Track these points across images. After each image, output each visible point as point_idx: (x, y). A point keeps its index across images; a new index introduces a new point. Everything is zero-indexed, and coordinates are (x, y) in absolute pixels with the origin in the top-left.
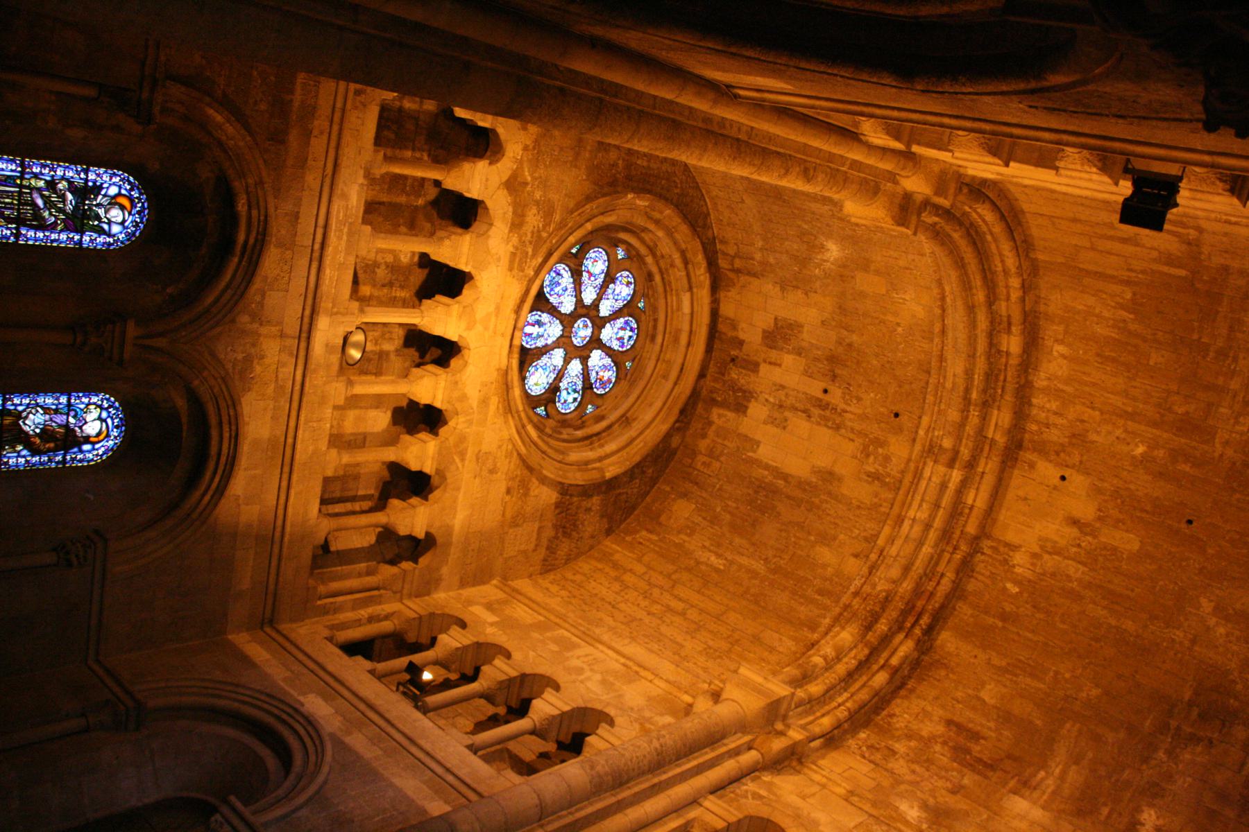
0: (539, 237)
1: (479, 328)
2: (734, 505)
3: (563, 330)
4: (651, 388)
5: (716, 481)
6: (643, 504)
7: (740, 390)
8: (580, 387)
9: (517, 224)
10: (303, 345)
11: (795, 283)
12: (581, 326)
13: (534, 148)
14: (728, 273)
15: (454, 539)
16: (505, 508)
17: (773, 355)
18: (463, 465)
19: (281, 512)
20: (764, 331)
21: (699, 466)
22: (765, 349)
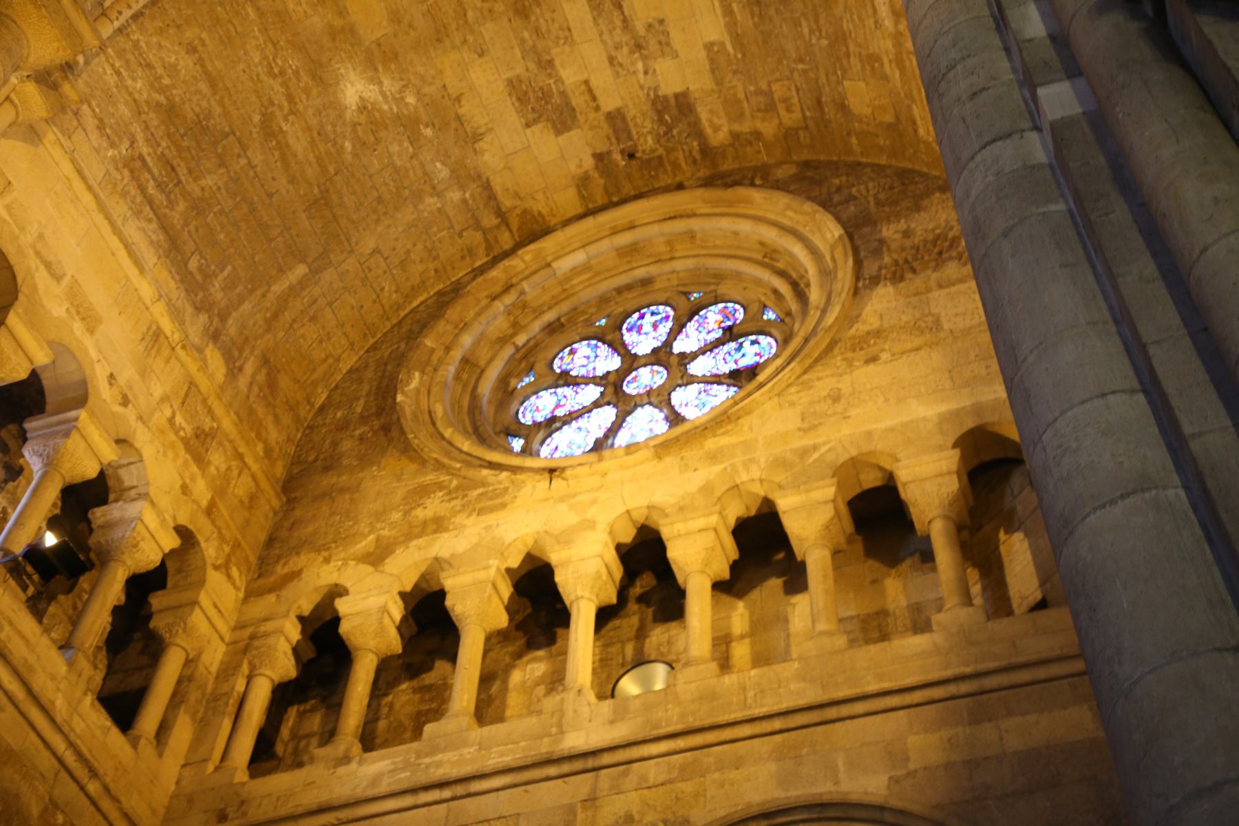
0: (457, 488)
1: (590, 514)
2: (804, 23)
3: (642, 406)
4: (715, 246)
5: (796, 75)
6: (894, 162)
7: (661, 121)
8: (733, 345)
9: (438, 525)
10: (607, 759)
11: (454, 124)
12: (635, 385)
13: (328, 549)
14: (515, 229)
15: (966, 402)
16: (903, 353)
17: (579, 101)
18: (824, 444)
19: (918, 696)
20: (558, 133)
21: (797, 115)
22: (581, 119)
